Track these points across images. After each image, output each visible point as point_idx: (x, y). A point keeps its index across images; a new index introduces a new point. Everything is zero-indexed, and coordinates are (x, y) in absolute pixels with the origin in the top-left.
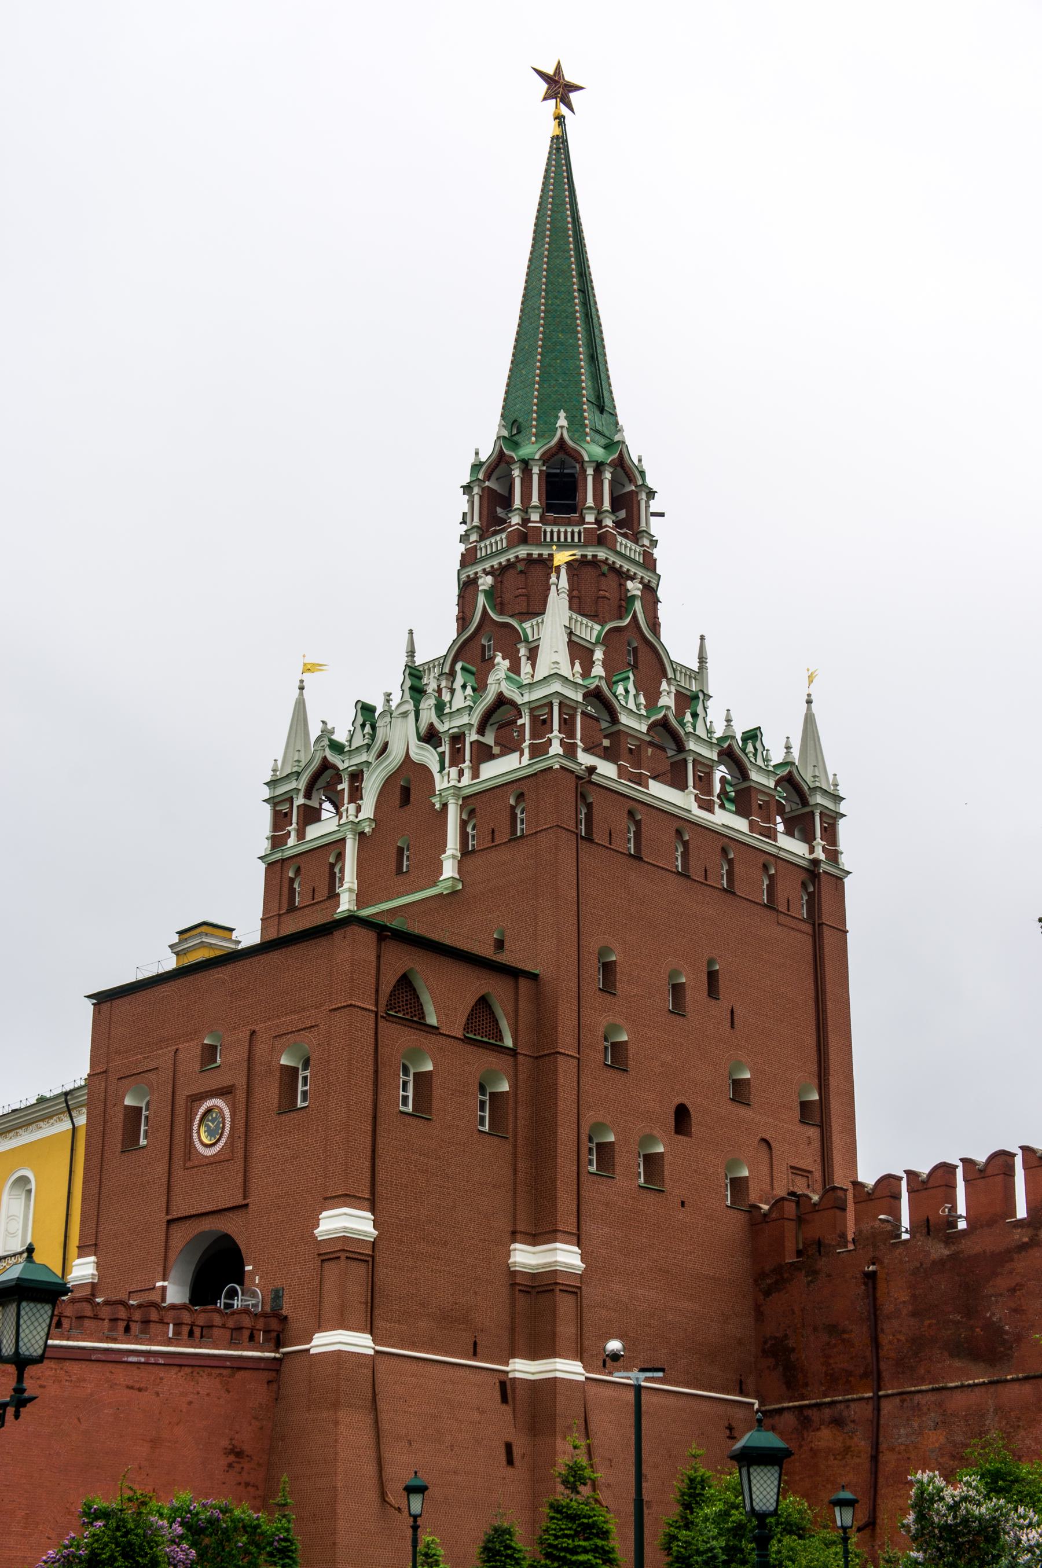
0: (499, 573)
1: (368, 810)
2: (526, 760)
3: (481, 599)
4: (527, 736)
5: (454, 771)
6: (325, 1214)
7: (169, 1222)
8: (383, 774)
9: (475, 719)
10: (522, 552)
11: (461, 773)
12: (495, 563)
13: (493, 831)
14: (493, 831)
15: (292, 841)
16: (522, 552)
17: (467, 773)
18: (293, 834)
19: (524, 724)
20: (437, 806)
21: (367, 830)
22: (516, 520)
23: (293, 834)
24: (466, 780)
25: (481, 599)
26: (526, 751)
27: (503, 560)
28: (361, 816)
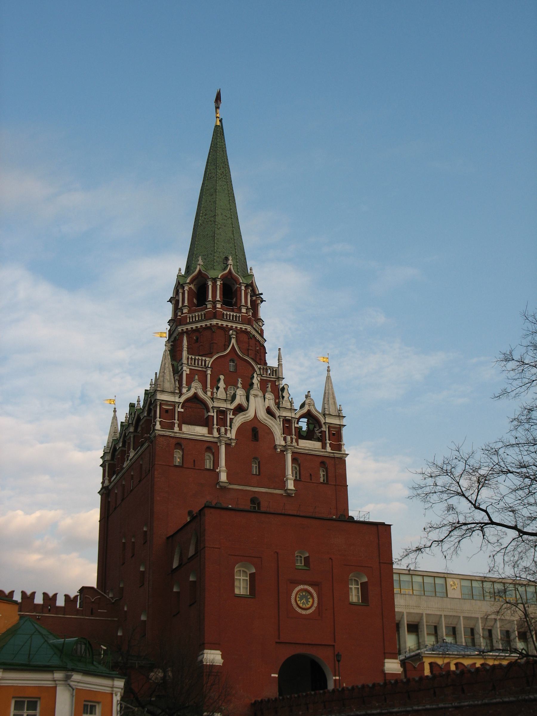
0: (240, 332)
1: (232, 434)
2: (329, 449)
3: (233, 341)
4: (327, 438)
5: (289, 438)
6: (386, 660)
7: (276, 642)
8: (243, 420)
9: (297, 416)
10: (249, 328)
11: (292, 439)
12: (234, 326)
13: (311, 475)
14: (311, 475)
15: (176, 429)
16: (249, 328)
17: (294, 441)
18: (176, 425)
19: (325, 431)
20: (279, 450)
21: (233, 444)
22: (244, 310)
23: (176, 425)
24: (294, 444)
25: (233, 341)
26: (328, 445)
27: (239, 326)
28: (229, 435)
